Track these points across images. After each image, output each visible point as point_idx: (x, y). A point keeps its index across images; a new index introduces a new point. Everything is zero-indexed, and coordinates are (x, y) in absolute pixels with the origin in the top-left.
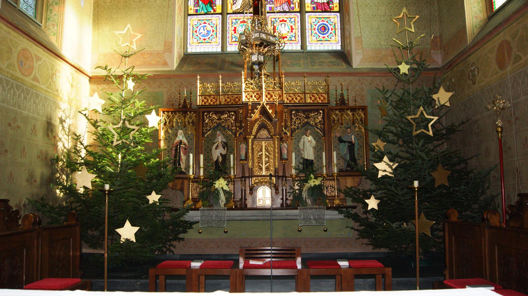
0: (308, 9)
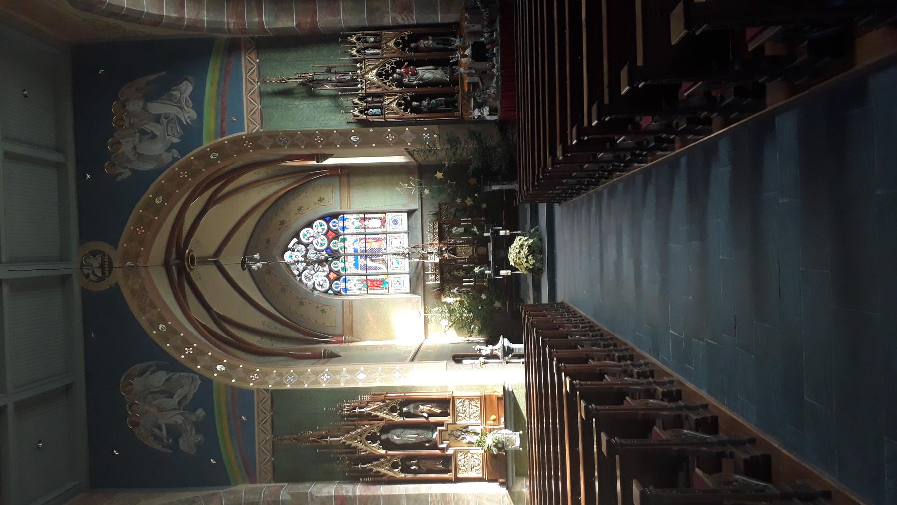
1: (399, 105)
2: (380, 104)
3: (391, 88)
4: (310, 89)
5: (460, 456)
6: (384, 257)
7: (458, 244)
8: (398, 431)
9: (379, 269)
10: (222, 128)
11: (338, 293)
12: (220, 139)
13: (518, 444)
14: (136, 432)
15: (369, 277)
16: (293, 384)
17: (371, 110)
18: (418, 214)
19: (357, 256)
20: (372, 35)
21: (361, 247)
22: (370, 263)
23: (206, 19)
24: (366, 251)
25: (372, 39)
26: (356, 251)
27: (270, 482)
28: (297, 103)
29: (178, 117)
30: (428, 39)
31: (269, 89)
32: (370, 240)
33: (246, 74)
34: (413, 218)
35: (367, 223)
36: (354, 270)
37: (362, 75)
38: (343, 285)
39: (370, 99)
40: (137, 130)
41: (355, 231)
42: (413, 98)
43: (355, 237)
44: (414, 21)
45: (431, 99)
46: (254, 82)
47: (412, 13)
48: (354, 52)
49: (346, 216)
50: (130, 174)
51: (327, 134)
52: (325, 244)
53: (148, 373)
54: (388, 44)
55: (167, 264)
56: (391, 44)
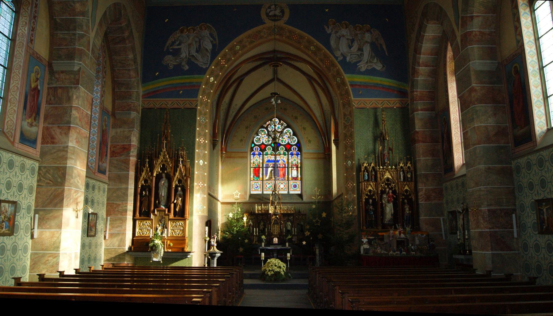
0: (290, 179)
1: (370, 191)
2: (370, 179)
3: (380, 186)
4: (379, 137)
5: (149, 222)
6: (274, 178)
7: (280, 226)
8: (166, 184)
9: (266, 175)
10: (356, 85)
11: (252, 149)
12: (348, 84)
13: (155, 259)
14: (177, 31)
15: (261, 169)
16: (199, 121)
17: (367, 174)
18: (300, 201)
19: (275, 162)
20: (412, 176)
21: (280, 164)
22: (270, 169)
23: (419, 79)
24: (277, 167)
25: (409, 176)
26: (278, 161)
27: (142, 106)
28: (371, 129)
29: (362, 60)
30: (409, 210)
31: (378, 114)
32: (284, 170)
33: (387, 100)
34: (298, 197)
35: (295, 168)
36: (266, 160)
37: (388, 169)
38: (257, 153)
39: (373, 173)
40: (354, 37)
41: (290, 161)
42: (374, 200)
43: (286, 160)
44: (421, 202)
45: (373, 211)
46: (383, 105)
47: (426, 201)
48: (401, 165)
49: (299, 156)
50: (328, 32)
51: (352, 147)
52: (282, 142)
53: (212, 39)
54: (406, 186)
55: (274, 51)
56: (406, 188)
